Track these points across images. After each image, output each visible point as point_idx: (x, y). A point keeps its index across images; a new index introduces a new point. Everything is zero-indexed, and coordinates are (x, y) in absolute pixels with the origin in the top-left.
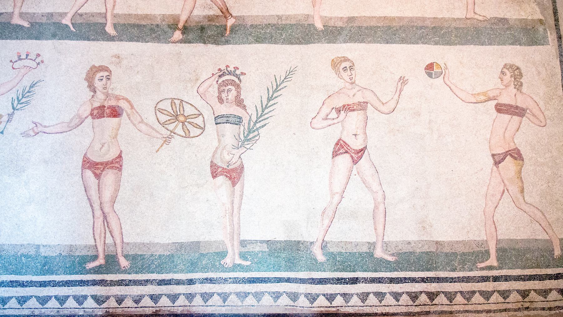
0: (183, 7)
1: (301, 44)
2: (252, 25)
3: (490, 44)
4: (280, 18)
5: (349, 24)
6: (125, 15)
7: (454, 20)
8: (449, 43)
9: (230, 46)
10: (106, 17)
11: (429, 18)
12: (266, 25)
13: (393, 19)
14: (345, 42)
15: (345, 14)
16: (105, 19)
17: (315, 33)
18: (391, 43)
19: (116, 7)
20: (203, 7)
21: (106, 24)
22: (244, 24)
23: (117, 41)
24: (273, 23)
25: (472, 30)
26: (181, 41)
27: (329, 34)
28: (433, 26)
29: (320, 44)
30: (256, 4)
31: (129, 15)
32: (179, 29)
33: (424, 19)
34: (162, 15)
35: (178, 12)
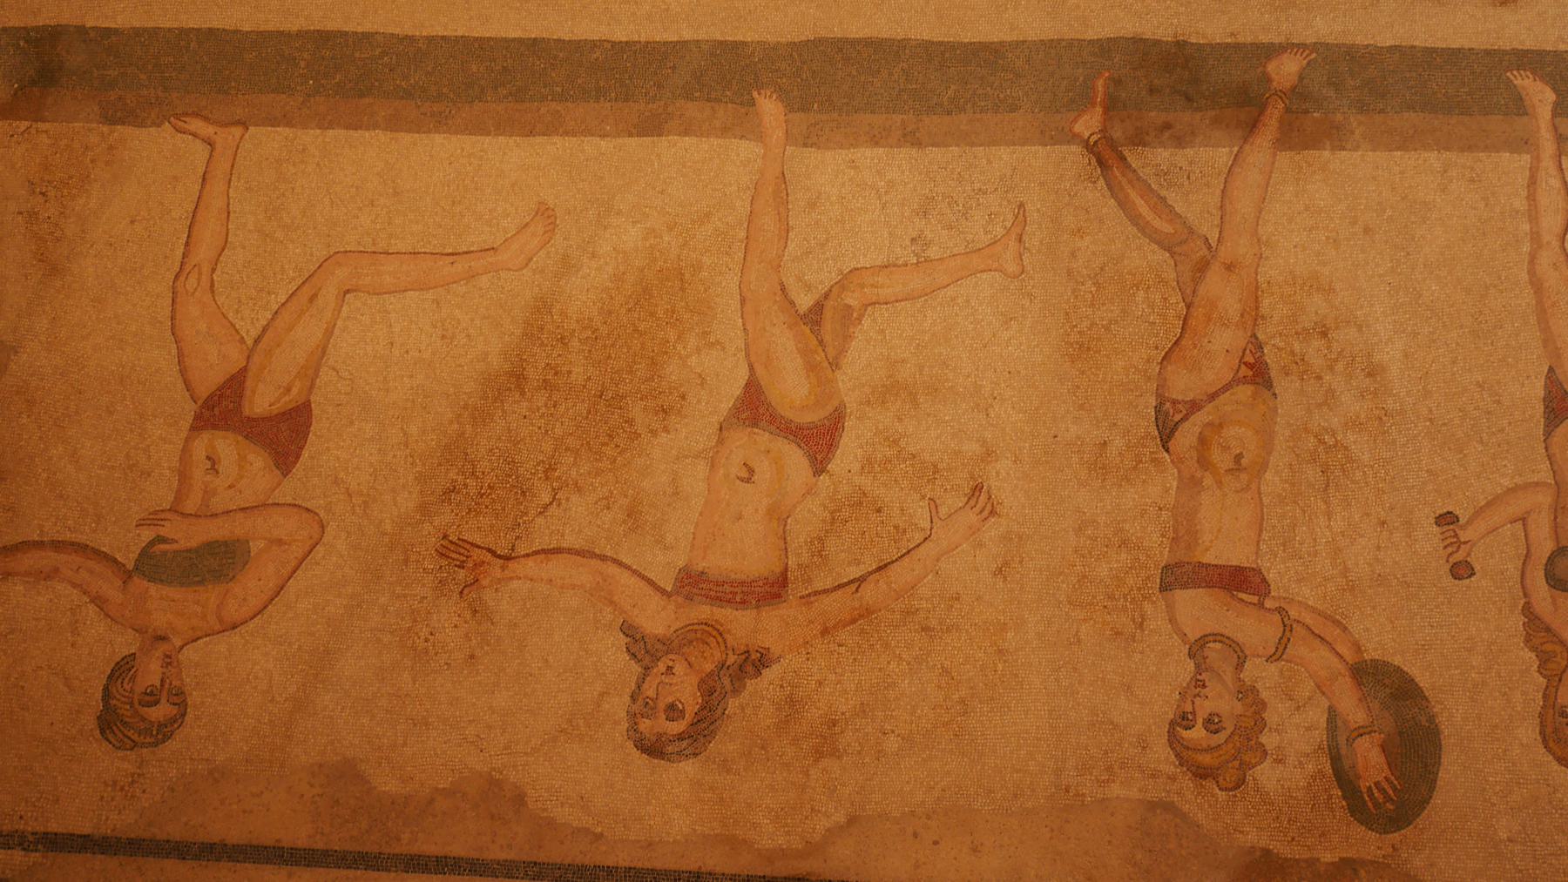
0: (1270, 177)
1: (840, 40)
2: (1014, 109)
3: (184, 32)
4: (912, 139)
5: (660, 110)
6: (1486, 149)
7: (287, 120)
8: (324, 38)
9: (1091, 35)
10: (1559, 138)
11: (375, 126)
12: (963, 110)
13: (503, 127)
14: (680, 46)
15: (674, 149)
16: (1561, 130)
17: (784, 80)
18: (520, 41)
19: (1522, 179)
20: (1193, 178)
21: (1555, 114)
22: (1043, 113)
23: (1505, 52)
24: (935, 117)
25: (233, 84)
26: (1272, 51)
27: (737, 77)
28: (367, 100)
29: (771, 39)
30: (996, 189)
31: (1470, 148)
32: (1281, 94)
33: (394, 124)
34: (1349, 146)
35: (1284, 158)
